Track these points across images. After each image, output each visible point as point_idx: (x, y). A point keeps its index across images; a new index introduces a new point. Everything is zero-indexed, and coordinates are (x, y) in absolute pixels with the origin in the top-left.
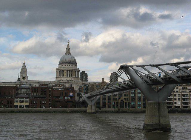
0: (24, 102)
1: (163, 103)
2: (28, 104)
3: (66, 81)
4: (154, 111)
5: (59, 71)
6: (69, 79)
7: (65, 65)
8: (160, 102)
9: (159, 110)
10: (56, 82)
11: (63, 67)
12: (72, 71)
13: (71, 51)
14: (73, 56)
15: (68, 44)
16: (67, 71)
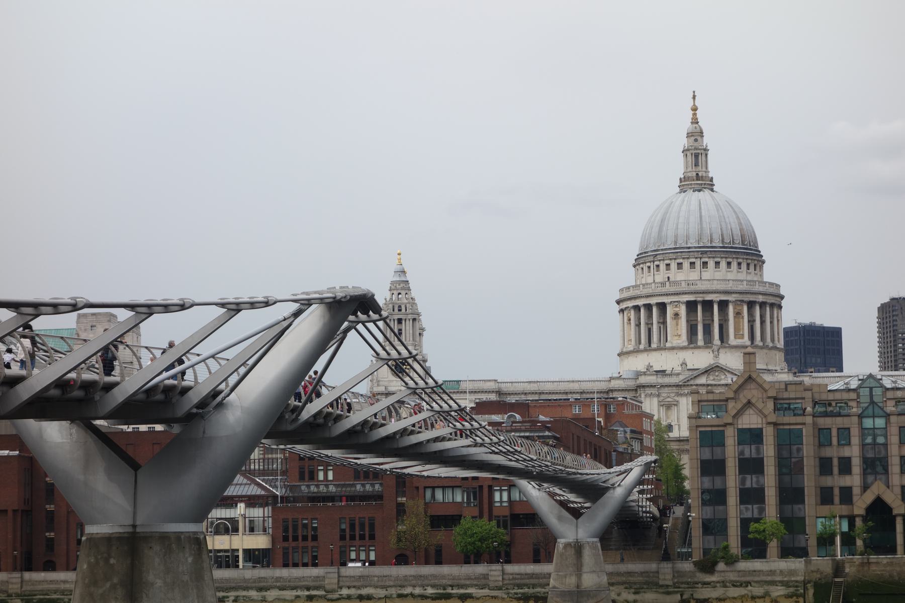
0: (236, 530)
1: (164, 537)
2: (260, 542)
3: (678, 374)
4: (101, 591)
5: (637, 308)
6: (700, 359)
7: (673, 265)
8: (138, 530)
9: (133, 586)
10: (615, 384)
11: (659, 278)
12: (723, 305)
13: (715, 167)
14: (729, 203)
15: (695, 121)
16: (691, 306)
